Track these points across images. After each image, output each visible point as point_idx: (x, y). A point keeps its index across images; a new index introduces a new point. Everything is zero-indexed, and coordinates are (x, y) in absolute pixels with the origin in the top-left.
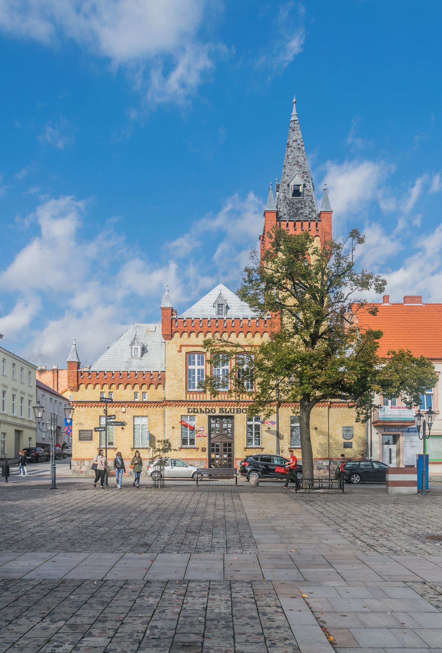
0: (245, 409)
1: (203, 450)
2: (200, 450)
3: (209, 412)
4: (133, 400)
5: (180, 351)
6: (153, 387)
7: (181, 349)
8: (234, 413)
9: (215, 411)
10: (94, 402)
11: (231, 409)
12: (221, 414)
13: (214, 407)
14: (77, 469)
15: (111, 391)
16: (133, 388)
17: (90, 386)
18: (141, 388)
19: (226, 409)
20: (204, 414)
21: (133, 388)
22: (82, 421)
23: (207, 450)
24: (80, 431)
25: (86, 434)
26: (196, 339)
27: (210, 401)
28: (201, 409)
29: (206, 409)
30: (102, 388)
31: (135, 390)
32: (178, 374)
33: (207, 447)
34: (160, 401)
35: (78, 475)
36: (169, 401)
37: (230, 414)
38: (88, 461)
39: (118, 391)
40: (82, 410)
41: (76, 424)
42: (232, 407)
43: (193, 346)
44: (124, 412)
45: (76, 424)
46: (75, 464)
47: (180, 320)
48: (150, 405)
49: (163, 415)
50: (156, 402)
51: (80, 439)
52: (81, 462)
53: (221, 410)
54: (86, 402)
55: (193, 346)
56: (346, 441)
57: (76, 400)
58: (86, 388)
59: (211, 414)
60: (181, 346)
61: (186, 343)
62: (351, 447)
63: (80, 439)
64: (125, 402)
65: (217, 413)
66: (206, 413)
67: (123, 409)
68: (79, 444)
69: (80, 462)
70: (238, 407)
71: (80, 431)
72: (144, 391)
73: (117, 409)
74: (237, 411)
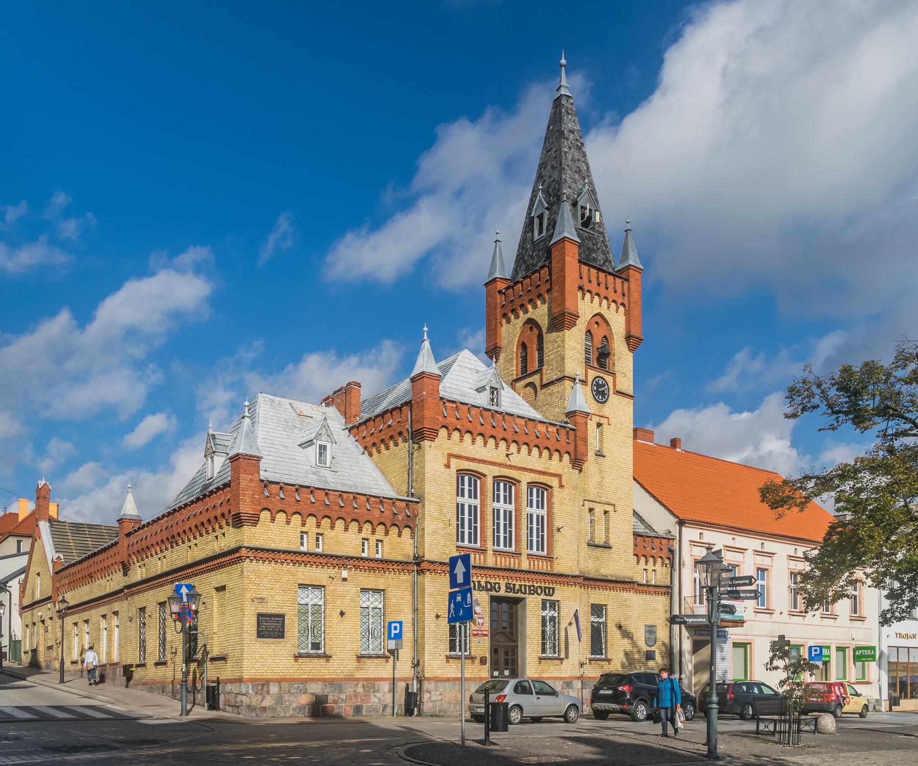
0: (541, 587)
1: (483, 661)
2: (477, 661)
3: (491, 590)
4: (359, 555)
5: (448, 466)
6: (394, 531)
7: (449, 462)
8: (525, 593)
9: (499, 588)
10: (289, 552)
11: (520, 586)
12: (508, 594)
13: (497, 581)
14: (254, 703)
15: (320, 531)
16: (360, 530)
17: (281, 517)
18: (373, 532)
19: (514, 585)
20: (484, 592)
21: (360, 530)
22: (264, 594)
23: (488, 660)
24: (259, 615)
25: (271, 625)
26: (471, 447)
27: (494, 569)
28: (479, 582)
29: (486, 583)
30: (303, 525)
31: (363, 535)
32: (445, 511)
33: (488, 655)
34: (405, 560)
35: (257, 716)
36: (433, 562)
37: (519, 595)
38: (277, 684)
39: (333, 533)
40: (265, 568)
41: (253, 601)
42: (523, 583)
43: (468, 459)
44: (345, 580)
45: (253, 601)
46: (251, 691)
47: (451, 405)
48: (390, 566)
49: (410, 590)
50: (401, 563)
51: (261, 634)
52: (263, 685)
53: (508, 587)
54: (273, 551)
55: (468, 459)
56: (649, 649)
57: (251, 545)
58: (273, 520)
59: (494, 593)
60: (450, 456)
61: (456, 451)
62: (653, 659)
63: (261, 634)
64: (347, 558)
65: (502, 593)
66: (487, 590)
67: (345, 574)
68: (258, 645)
69: (260, 688)
70: (531, 584)
71: (259, 615)
72: (379, 538)
73: (332, 572)
74: (530, 590)
